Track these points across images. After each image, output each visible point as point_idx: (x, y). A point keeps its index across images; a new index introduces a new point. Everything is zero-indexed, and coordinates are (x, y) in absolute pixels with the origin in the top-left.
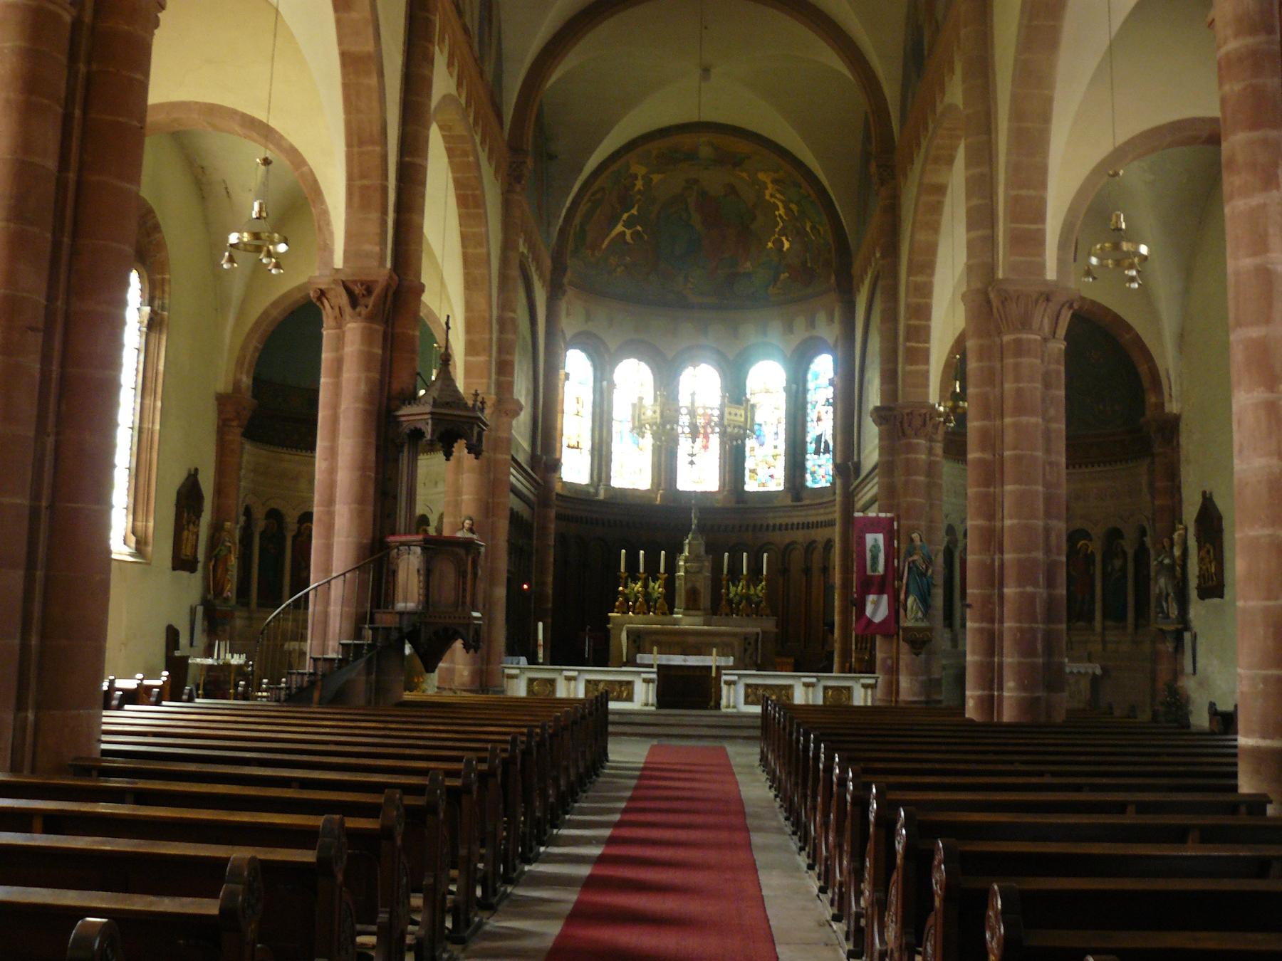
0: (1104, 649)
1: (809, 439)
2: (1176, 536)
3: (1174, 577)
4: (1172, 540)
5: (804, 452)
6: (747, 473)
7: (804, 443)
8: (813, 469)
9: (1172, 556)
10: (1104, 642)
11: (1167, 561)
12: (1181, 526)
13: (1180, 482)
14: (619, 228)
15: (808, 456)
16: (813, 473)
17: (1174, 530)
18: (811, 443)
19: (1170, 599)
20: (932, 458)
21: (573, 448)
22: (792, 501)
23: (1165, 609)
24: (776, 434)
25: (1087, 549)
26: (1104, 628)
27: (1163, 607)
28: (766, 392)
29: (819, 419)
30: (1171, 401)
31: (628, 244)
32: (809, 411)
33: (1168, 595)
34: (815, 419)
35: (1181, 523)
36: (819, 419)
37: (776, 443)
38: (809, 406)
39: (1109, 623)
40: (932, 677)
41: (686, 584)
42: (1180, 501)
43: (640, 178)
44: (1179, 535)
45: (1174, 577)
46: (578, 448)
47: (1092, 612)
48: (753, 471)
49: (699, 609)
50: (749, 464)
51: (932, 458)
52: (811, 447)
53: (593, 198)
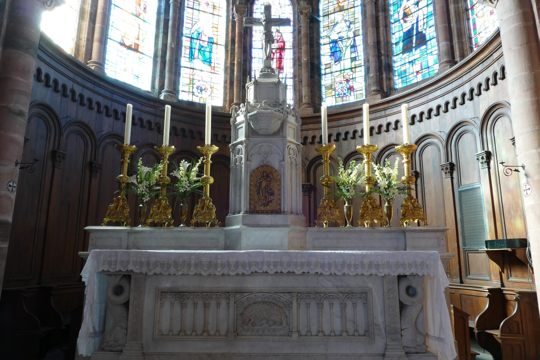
1: (394, 41)
5: (389, 54)
6: (323, 89)
7: (388, 44)
8: (403, 68)
15: (395, 58)
16: (403, 75)
18: (397, 44)
21: (129, 48)
22: (383, 97)
24: (354, 46)
28: (340, 11)
29: (406, 15)
32: (392, 13)
34: (401, 17)
36: (406, 15)
37: (353, 55)
38: (392, 8)
41: (247, 159)
46: (136, 50)
48: (330, 87)
49: (278, 212)
50: (325, 81)
52: (397, 49)
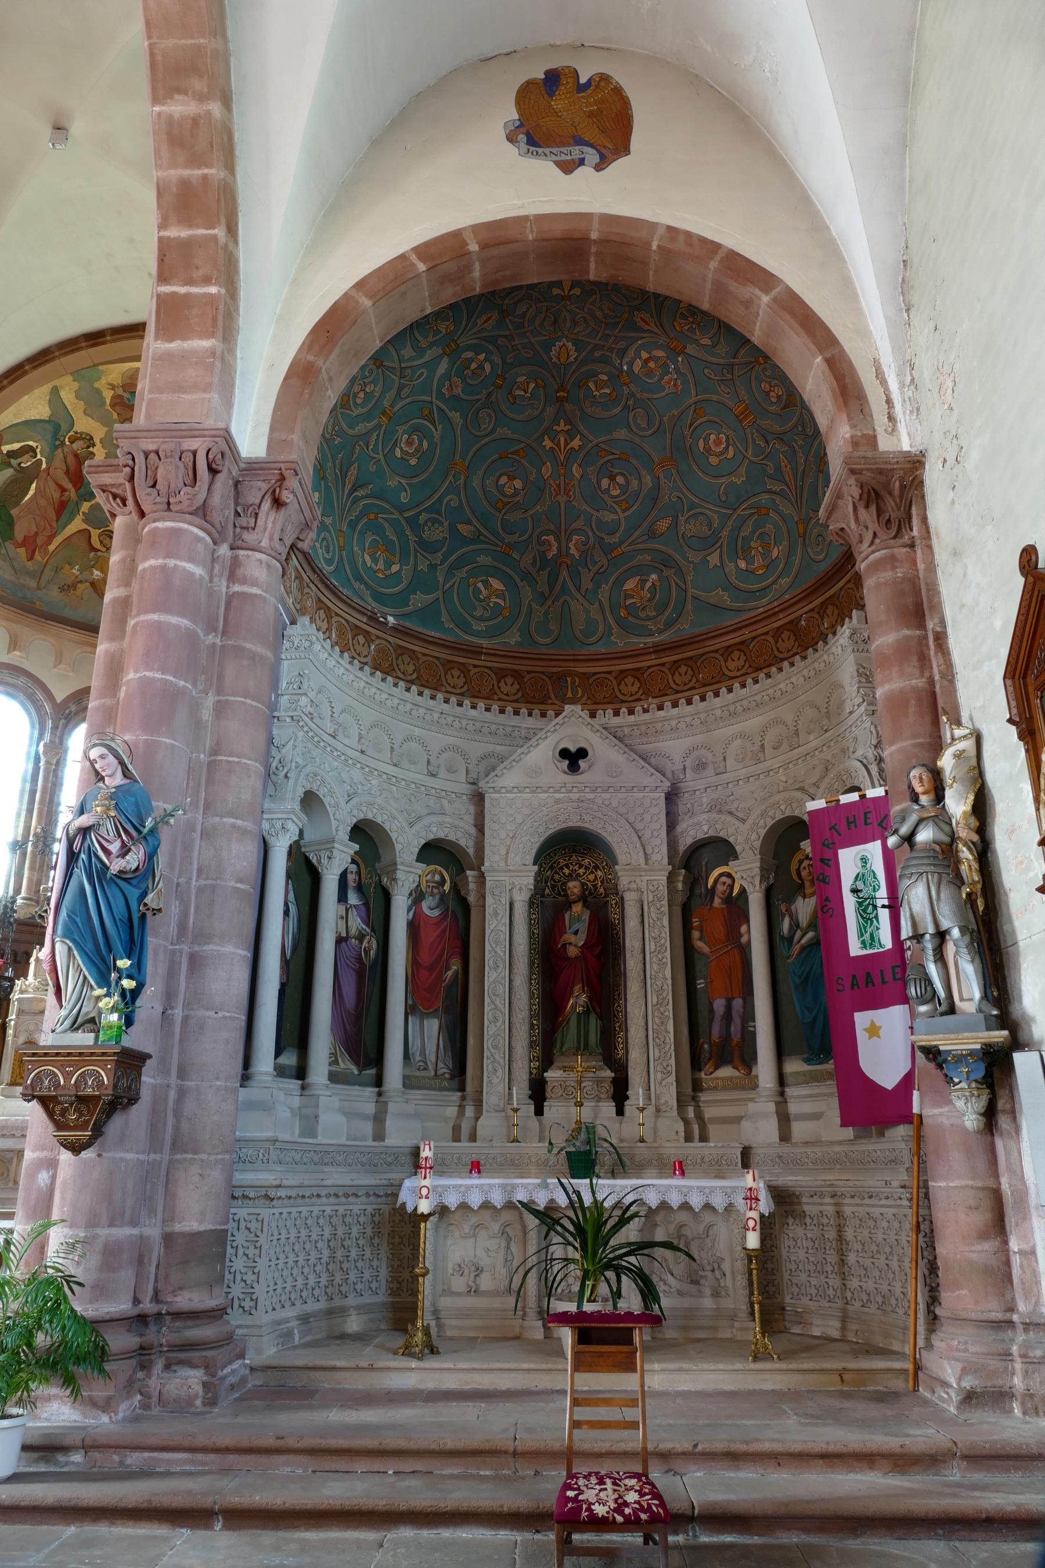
0: (785, 1136)
2: (946, 762)
3: (958, 880)
4: (936, 775)
9: (942, 818)
10: (784, 1119)
11: (924, 836)
12: (958, 732)
13: (943, 622)
14: (77, 524)
17: (937, 747)
19: (950, 949)
20: (237, 588)
23: (942, 993)
25: (732, 887)
26: (782, 1080)
27: (929, 982)
30: (893, 431)
31: (97, 550)
33: (941, 935)
35: (959, 723)
39: (794, 1066)
40: (178, 1227)
42: (949, 673)
43: (97, 441)
44: (959, 756)
45: (958, 880)
47: (749, 1039)
51: (237, 588)
53: (14, 462)
